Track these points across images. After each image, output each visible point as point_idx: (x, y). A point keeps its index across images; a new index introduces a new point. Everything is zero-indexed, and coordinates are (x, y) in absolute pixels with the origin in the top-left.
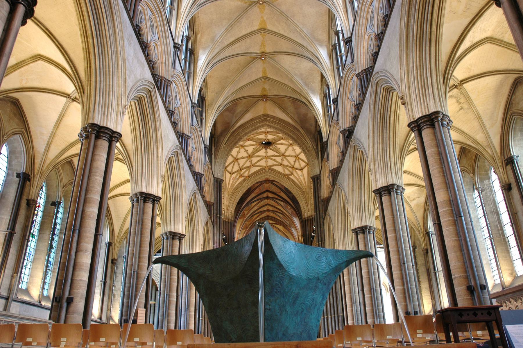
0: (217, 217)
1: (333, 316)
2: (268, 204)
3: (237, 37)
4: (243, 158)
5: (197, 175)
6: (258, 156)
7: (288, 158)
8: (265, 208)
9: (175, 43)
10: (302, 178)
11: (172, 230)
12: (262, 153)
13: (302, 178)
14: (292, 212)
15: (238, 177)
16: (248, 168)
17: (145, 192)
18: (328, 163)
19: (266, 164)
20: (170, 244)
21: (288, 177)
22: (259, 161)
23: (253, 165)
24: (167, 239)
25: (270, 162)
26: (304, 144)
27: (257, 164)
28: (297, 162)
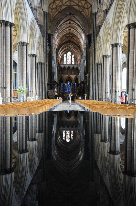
0: (45, 33)
1: (96, 83)
5: (34, 10)
11: (22, 41)
14: (81, 31)
15: (55, 11)
16: (61, 6)
17: (5, 20)
18: (103, 6)
19: (70, 5)
20: (21, 48)
21: (81, 12)
23: (63, 5)
24: (20, 45)
27: (65, 4)
28: (86, 5)
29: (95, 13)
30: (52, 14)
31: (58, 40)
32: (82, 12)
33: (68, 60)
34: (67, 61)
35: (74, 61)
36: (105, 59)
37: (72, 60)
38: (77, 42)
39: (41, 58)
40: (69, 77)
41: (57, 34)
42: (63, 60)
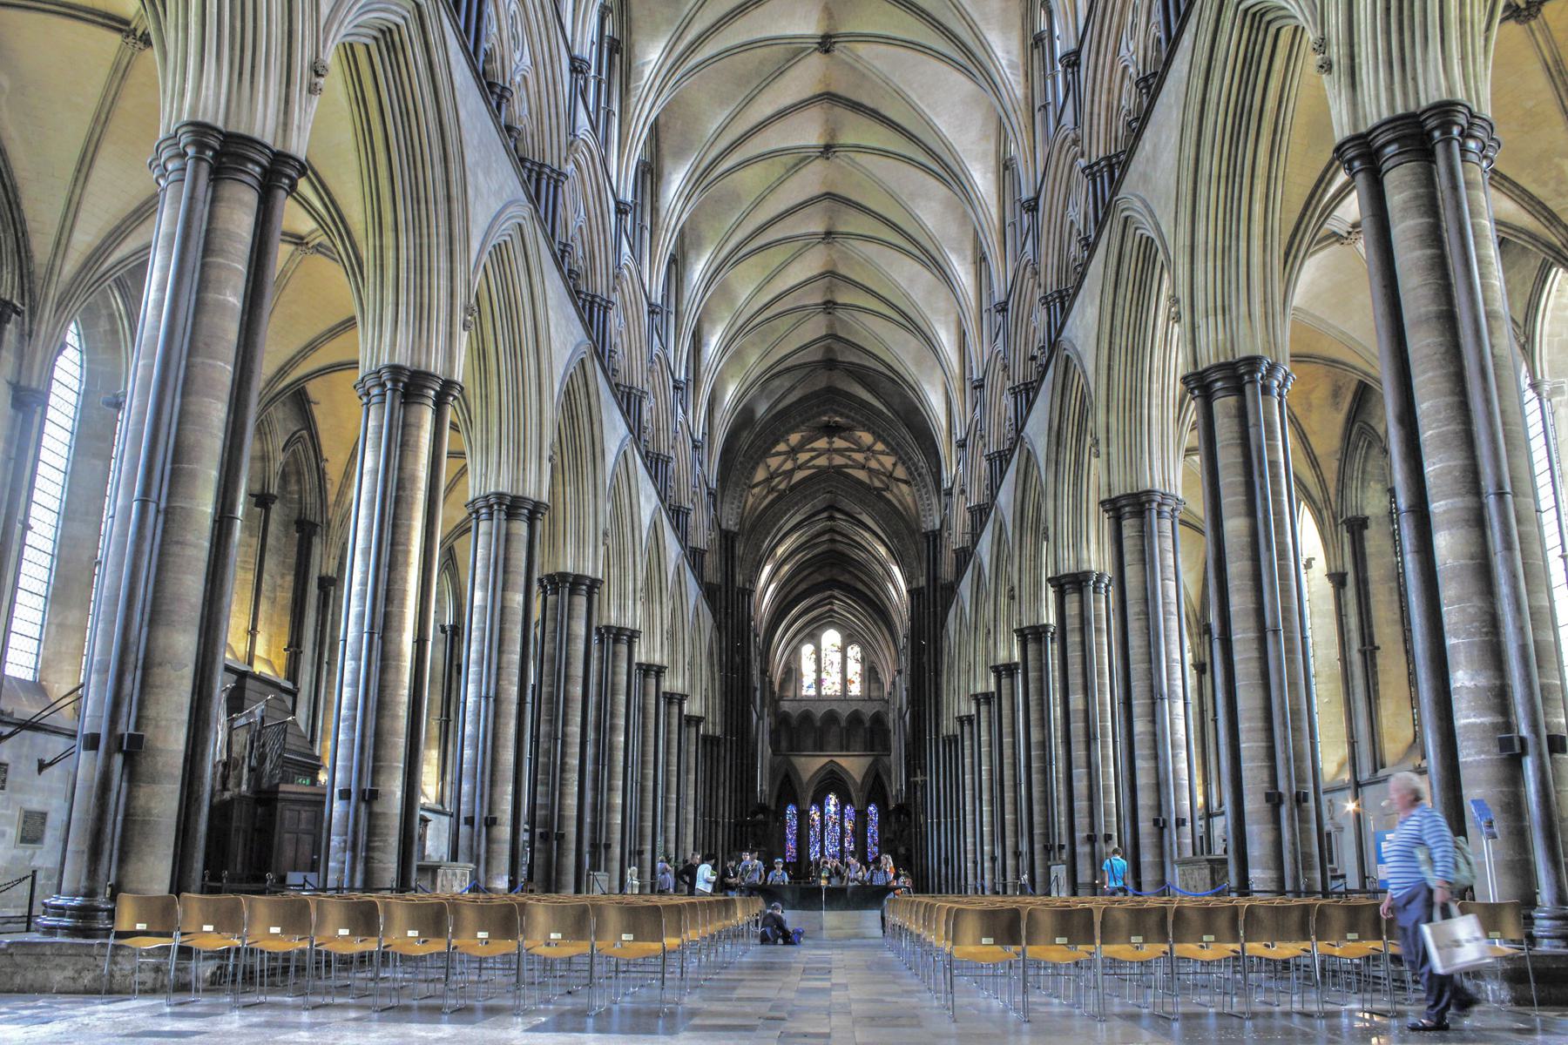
0: (727, 614)
2: (832, 530)
3: (777, 292)
4: (779, 454)
6: (813, 450)
7: (881, 457)
8: (825, 537)
9: (674, 381)
10: (909, 499)
12: (822, 443)
13: (909, 499)
16: (790, 473)
22: (812, 458)
23: (800, 468)
25: (839, 460)
26: (911, 459)
29: (933, 532)
30: (751, 500)
31: (772, 587)
32: (888, 495)
33: (824, 675)
34: (819, 682)
35: (857, 679)
36: (967, 729)
37: (850, 676)
38: (873, 591)
39: (714, 727)
40: (832, 772)
41: (767, 570)
42: (801, 675)
